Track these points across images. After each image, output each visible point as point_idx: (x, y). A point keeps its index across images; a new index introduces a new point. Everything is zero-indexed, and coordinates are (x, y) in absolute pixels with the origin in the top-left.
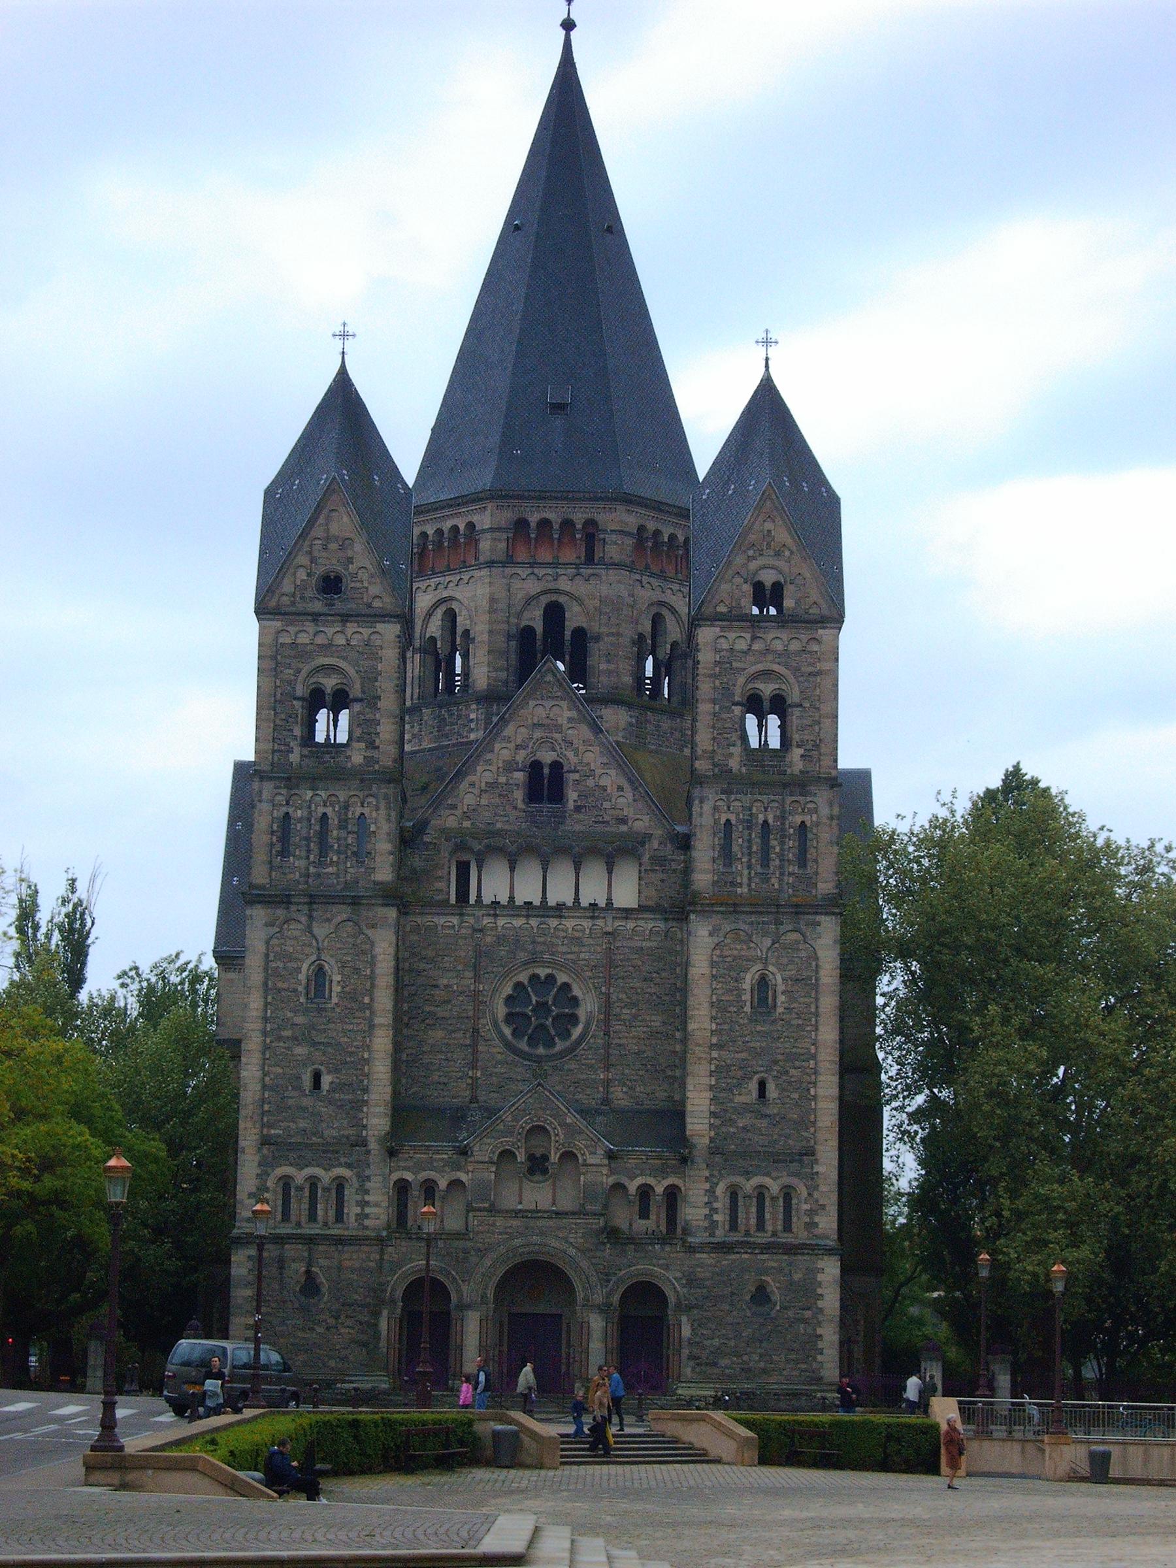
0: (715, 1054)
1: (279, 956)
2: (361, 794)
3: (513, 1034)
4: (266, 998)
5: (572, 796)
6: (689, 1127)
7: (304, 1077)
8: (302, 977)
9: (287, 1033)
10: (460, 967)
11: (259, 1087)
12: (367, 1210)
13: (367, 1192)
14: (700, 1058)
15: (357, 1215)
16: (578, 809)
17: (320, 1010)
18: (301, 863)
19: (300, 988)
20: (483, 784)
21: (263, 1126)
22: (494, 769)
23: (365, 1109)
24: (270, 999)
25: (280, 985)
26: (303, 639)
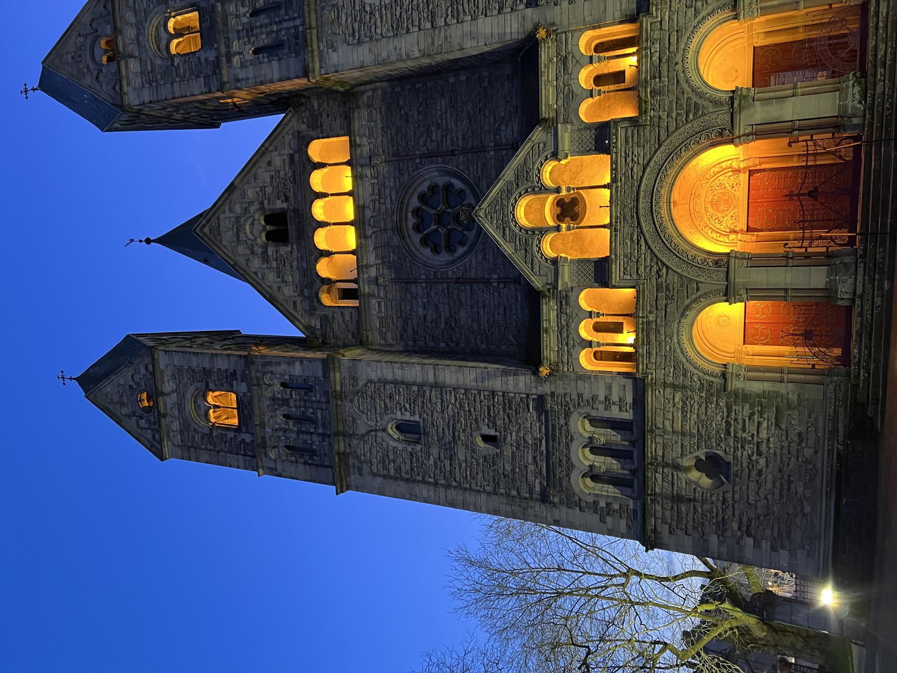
0: (440, 22)
1: (384, 467)
2: (264, 387)
3: (463, 245)
4: (419, 481)
5: (280, 205)
6: (515, 36)
7: (485, 453)
8: (400, 446)
9: (447, 463)
10: (409, 296)
11: (495, 498)
12: (615, 398)
13: (594, 398)
14: (446, 38)
15: (620, 410)
16: (287, 199)
17: (427, 434)
18: (315, 438)
19: (409, 449)
20: (279, 280)
21: (532, 499)
22: (267, 271)
23: (512, 395)
24: (420, 478)
25: (408, 467)
26: (176, 426)
